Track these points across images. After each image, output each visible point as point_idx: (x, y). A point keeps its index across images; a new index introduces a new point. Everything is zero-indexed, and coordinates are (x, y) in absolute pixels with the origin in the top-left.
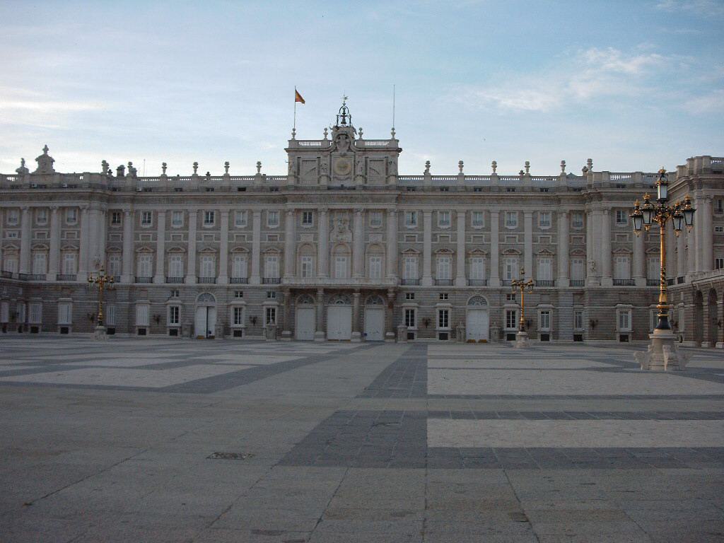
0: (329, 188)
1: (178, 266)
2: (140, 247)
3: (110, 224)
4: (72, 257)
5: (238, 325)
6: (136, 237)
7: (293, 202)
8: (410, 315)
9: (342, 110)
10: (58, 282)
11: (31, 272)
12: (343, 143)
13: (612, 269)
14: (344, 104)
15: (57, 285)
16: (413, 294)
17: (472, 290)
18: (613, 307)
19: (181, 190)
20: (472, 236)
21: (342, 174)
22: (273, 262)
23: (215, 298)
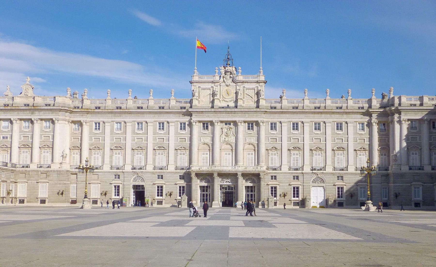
0: (220, 108)
1: (119, 158)
2: (93, 146)
3: (73, 130)
4: (47, 152)
5: (160, 197)
6: (91, 139)
7: (196, 116)
8: (274, 191)
9: (227, 56)
10: (38, 169)
11: (19, 162)
12: (228, 77)
13: (408, 160)
14: (228, 52)
15: (37, 171)
16: (275, 177)
17: (315, 173)
18: (409, 184)
19: (120, 108)
20: (314, 139)
21: (228, 97)
22: (183, 156)
23: (145, 180)
